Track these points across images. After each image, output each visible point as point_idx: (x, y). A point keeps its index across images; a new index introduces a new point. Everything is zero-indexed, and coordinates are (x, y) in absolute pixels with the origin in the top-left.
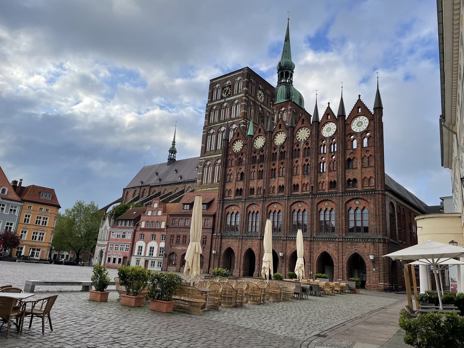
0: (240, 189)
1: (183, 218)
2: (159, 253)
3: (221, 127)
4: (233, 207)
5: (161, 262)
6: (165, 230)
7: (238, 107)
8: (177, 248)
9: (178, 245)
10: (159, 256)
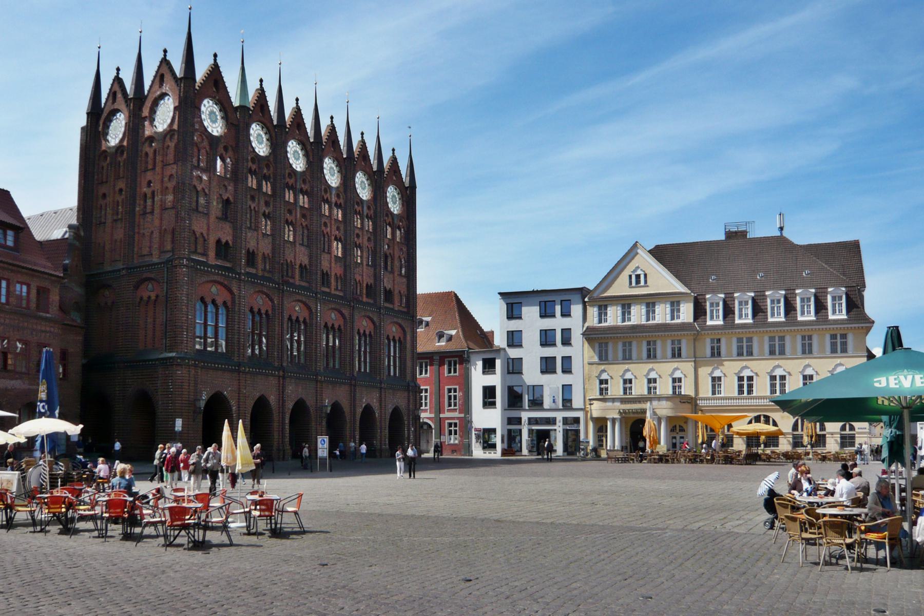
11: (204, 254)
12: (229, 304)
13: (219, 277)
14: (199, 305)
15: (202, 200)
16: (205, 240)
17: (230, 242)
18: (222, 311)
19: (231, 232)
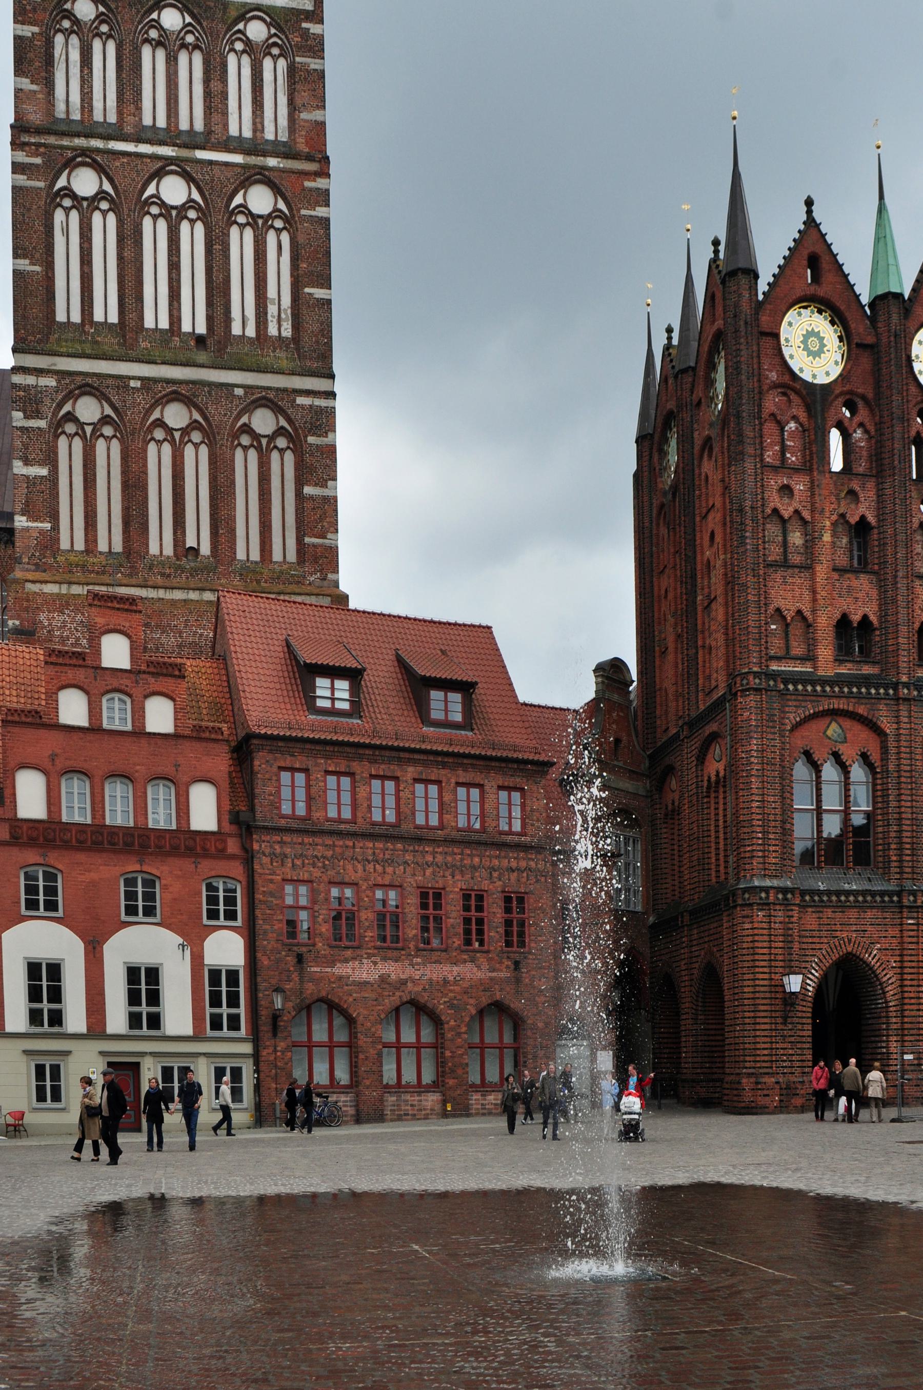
0: (859, 623)
1: (356, 767)
2: (208, 1010)
3: (159, 174)
4: (834, 726)
5: (236, 1074)
6: (233, 847)
7: (268, 76)
8: (341, 969)
9: (349, 953)
10: (209, 1033)
11: (810, 657)
12: (875, 757)
13: (844, 700)
14: (801, 770)
15: (796, 538)
16: (809, 626)
17: (873, 618)
18: (858, 773)
19: (874, 593)
